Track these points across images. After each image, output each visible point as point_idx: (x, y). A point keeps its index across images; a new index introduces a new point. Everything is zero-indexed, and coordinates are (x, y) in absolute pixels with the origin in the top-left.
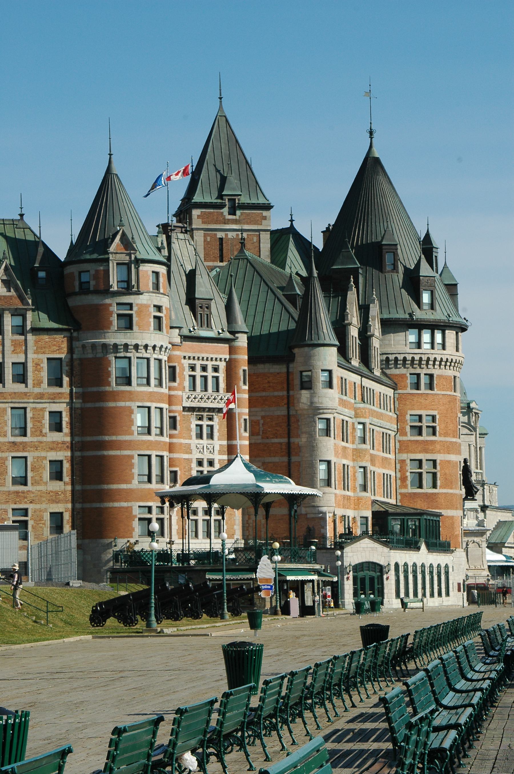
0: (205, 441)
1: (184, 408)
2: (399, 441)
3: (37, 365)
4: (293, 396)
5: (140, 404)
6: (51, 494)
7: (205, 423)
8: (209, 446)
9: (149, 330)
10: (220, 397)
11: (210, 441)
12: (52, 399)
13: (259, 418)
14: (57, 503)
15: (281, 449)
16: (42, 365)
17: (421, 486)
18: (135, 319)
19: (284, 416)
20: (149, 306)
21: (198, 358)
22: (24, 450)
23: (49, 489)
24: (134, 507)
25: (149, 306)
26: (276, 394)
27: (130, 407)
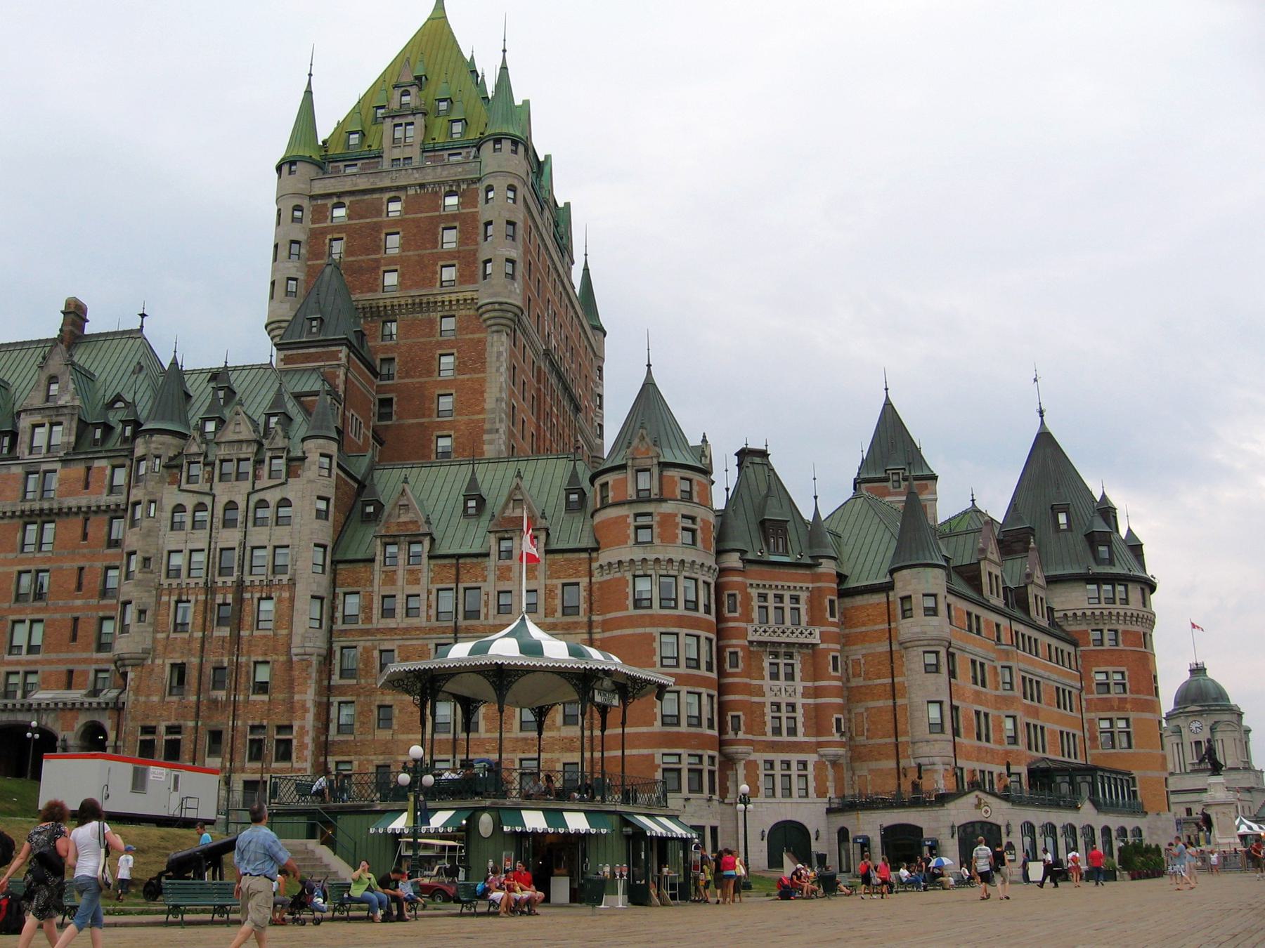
0: (782, 683)
1: (751, 642)
2: (1086, 700)
4: (895, 628)
5: (664, 630)
7: (782, 661)
9: (675, 543)
10: (799, 631)
11: (790, 683)
12: (566, 630)
13: (860, 657)
14: (572, 751)
16: (556, 592)
17: (1113, 747)
18: (656, 530)
19: (887, 652)
20: (676, 515)
21: (770, 586)
23: (562, 735)
25: (676, 515)
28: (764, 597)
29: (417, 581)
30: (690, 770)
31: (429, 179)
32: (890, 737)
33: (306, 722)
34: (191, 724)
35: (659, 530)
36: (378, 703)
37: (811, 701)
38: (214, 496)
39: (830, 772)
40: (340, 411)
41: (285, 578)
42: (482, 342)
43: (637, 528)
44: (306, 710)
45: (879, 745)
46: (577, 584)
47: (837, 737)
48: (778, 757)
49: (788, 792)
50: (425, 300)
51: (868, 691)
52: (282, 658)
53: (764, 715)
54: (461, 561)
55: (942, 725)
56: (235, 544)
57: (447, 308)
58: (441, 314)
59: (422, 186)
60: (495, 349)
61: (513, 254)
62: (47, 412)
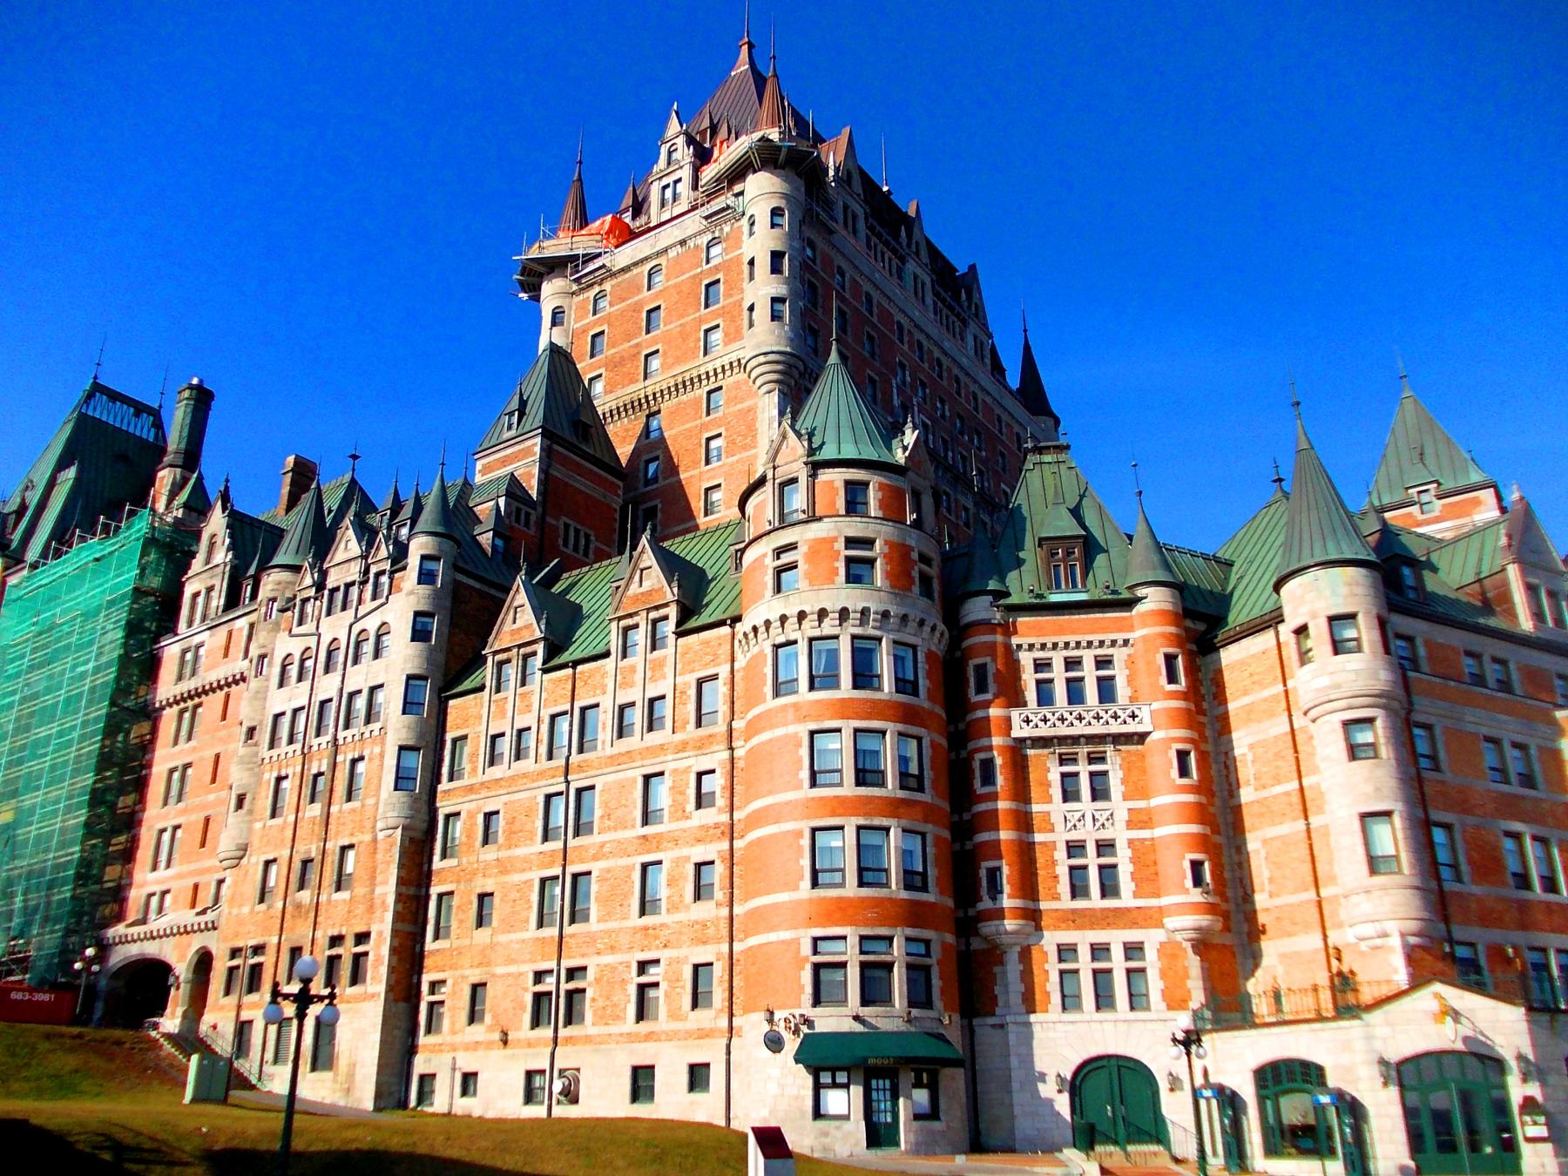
0: (1086, 804)
1: (1022, 740)
3: (683, 693)
4: (1294, 688)
5: (814, 726)
6: (697, 927)
8: (1097, 815)
9: (833, 583)
11: (1100, 805)
14: (705, 943)
15: (1291, 805)
19: (1286, 734)
20: (835, 539)
21: (1055, 646)
22: (658, 849)
24: (802, 940)
26: (1267, 693)
27: (796, 735)
28: (1041, 665)
29: (528, 708)
30: (909, 967)
31: (689, 232)
32: (1306, 890)
33: (383, 928)
34: (275, 940)
35: (806, 567)
36: (479, 890)
37: (1144, 834)
38: (319, 636)
39: (1194, 963)
40: (533, 518)
41: (375, 726)
42: (751, 410)
43: (779, 572)
44: (386, 910)
45: (1291, 905)
46: (714, 677)
47: (1196, 895)
48: (1083, 939)
49: (1104, 1000)
50: (687, 378)
51: (1264, 810)
52: (367, 838)
53: (1054, 863)
54: (580, 668)
55: (1397, 857)
56: (334, 693)
57: (713, 379)
58: (708, 389)
59: (683, 243)
60: (766, 415)
61: (781, 290)
62: (204, 575)
